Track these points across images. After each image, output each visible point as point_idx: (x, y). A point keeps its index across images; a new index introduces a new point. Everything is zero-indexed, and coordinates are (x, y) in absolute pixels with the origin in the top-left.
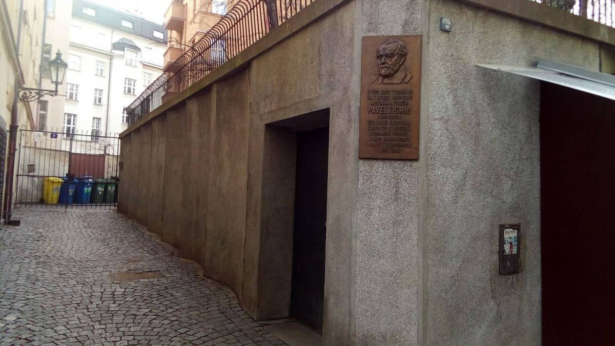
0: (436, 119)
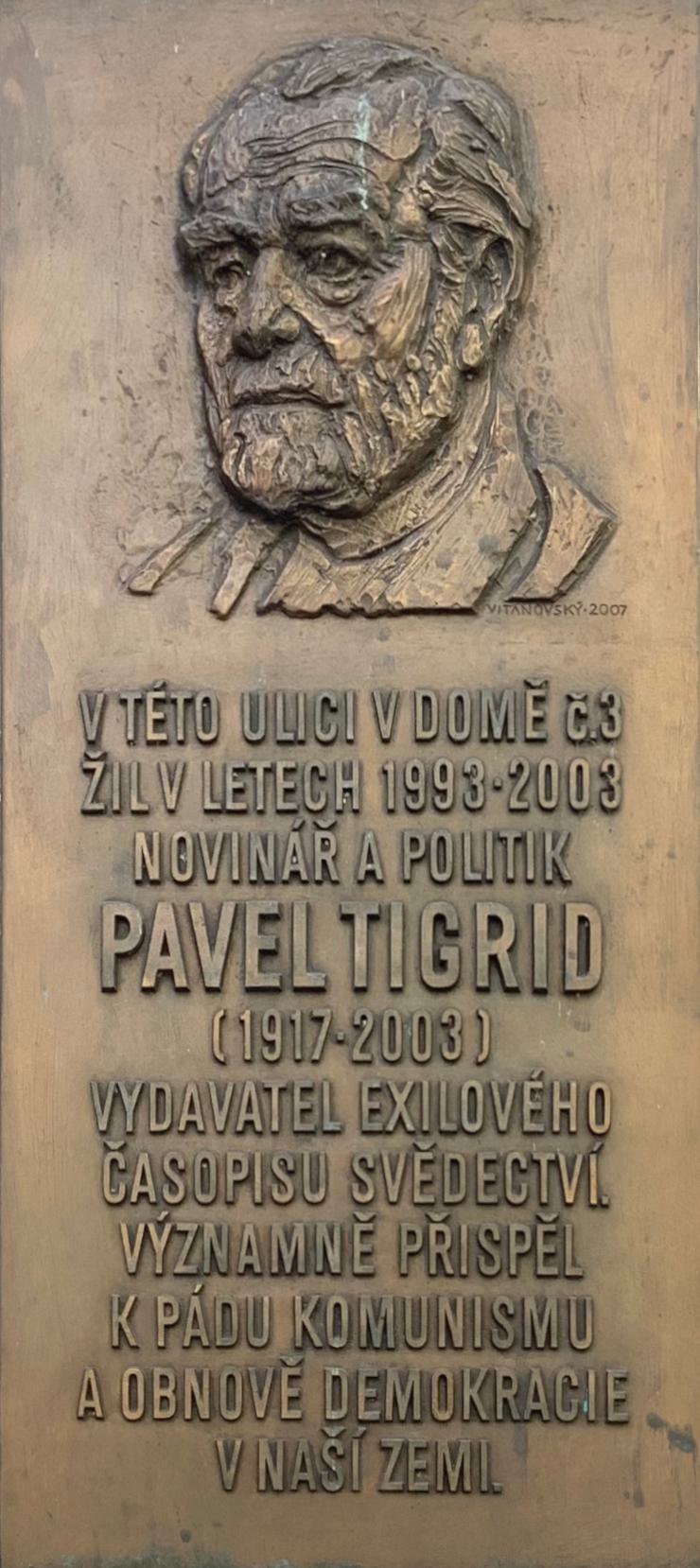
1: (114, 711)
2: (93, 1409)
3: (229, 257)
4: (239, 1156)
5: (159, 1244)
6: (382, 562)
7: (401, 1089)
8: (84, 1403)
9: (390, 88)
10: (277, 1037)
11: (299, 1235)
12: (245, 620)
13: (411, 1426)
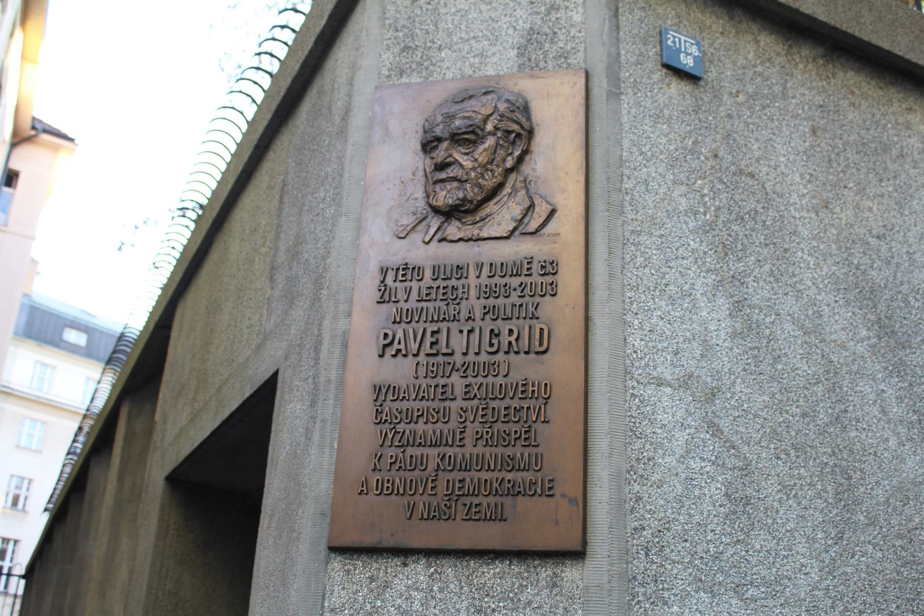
0: (660, 383)
1: (390, 271)
2: (363, 491)
3: (434, 144)
5: (390, 436)
6: (479, 225)
7: (476, 385)
8: (361, 489)
11: (438, 432)
12: (434, 243)
13: (474, 497)
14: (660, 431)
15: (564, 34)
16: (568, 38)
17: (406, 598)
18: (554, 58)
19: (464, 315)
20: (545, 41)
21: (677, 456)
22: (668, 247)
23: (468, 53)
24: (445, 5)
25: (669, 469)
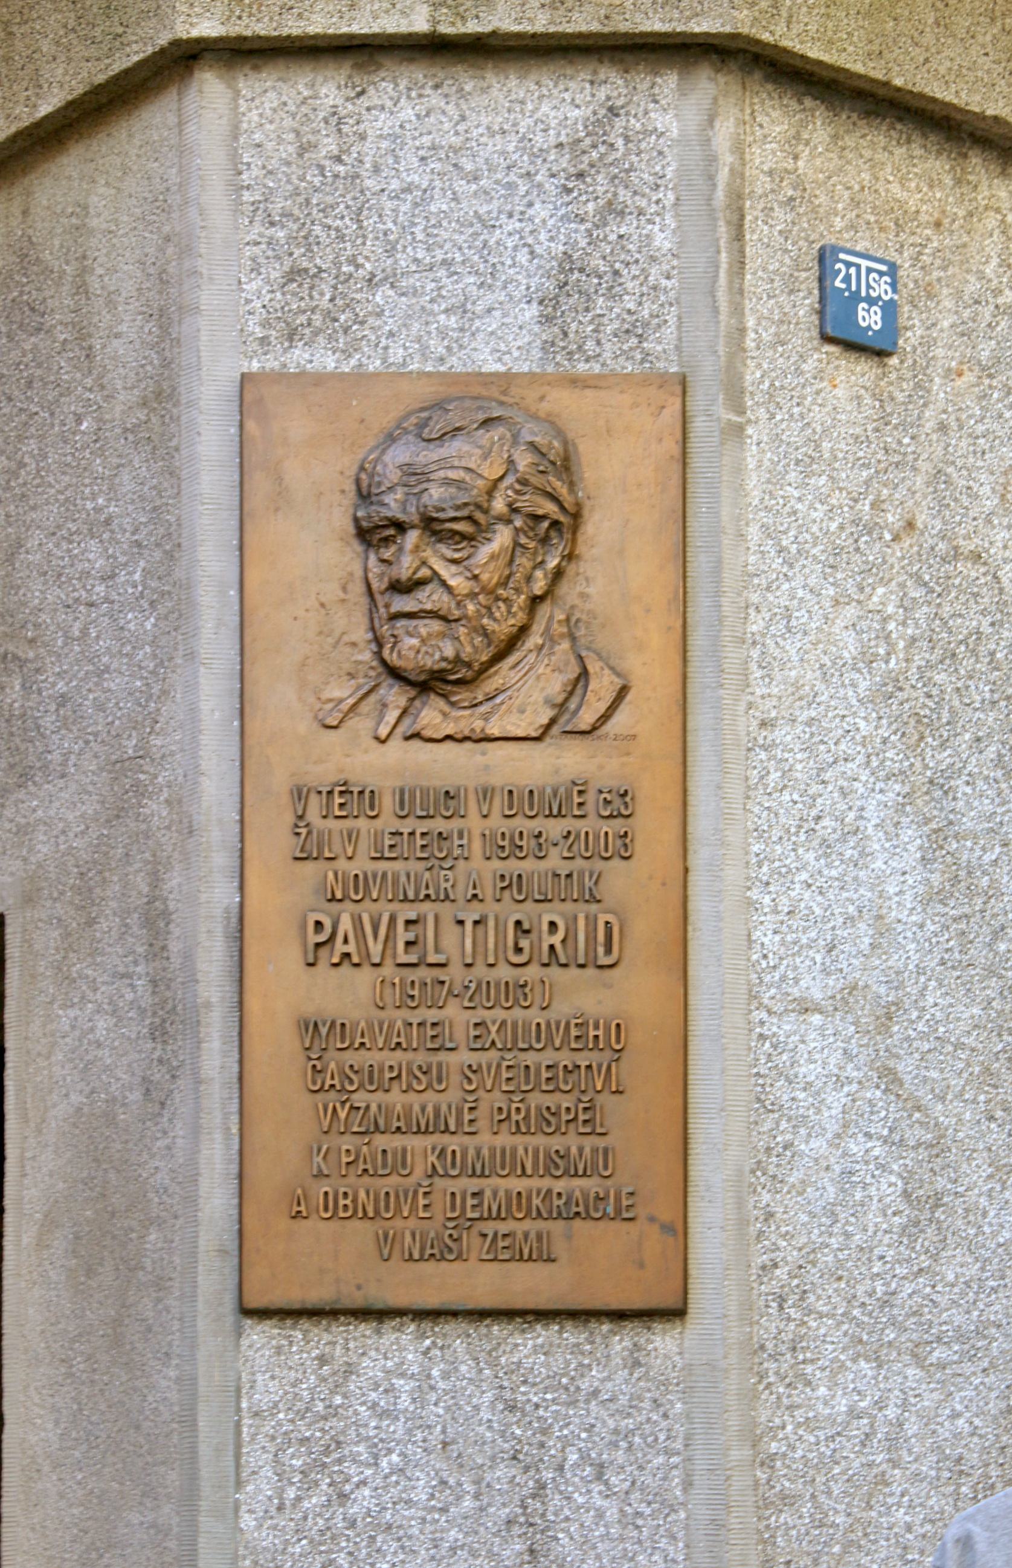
0: (805, 1008)
1: (314, 799)
4: (392, 1063)
5: (342, 1115)
6: (482, 709)
8: (296, 1208)
9: (488, 435)
10: (416, 993)
11: (430, 1109)
12: (396, 743)
14: (802, 1095)
15: (634, 277)
16: (645, 289)
17: (386, 1391)
18: (616, 335)
19: (461, 892)
20: (596, 291)
21: (829, 1135)
22: (822, 742)
23: (432, 301)
24: (376, 169)
25: (816, 1160)
